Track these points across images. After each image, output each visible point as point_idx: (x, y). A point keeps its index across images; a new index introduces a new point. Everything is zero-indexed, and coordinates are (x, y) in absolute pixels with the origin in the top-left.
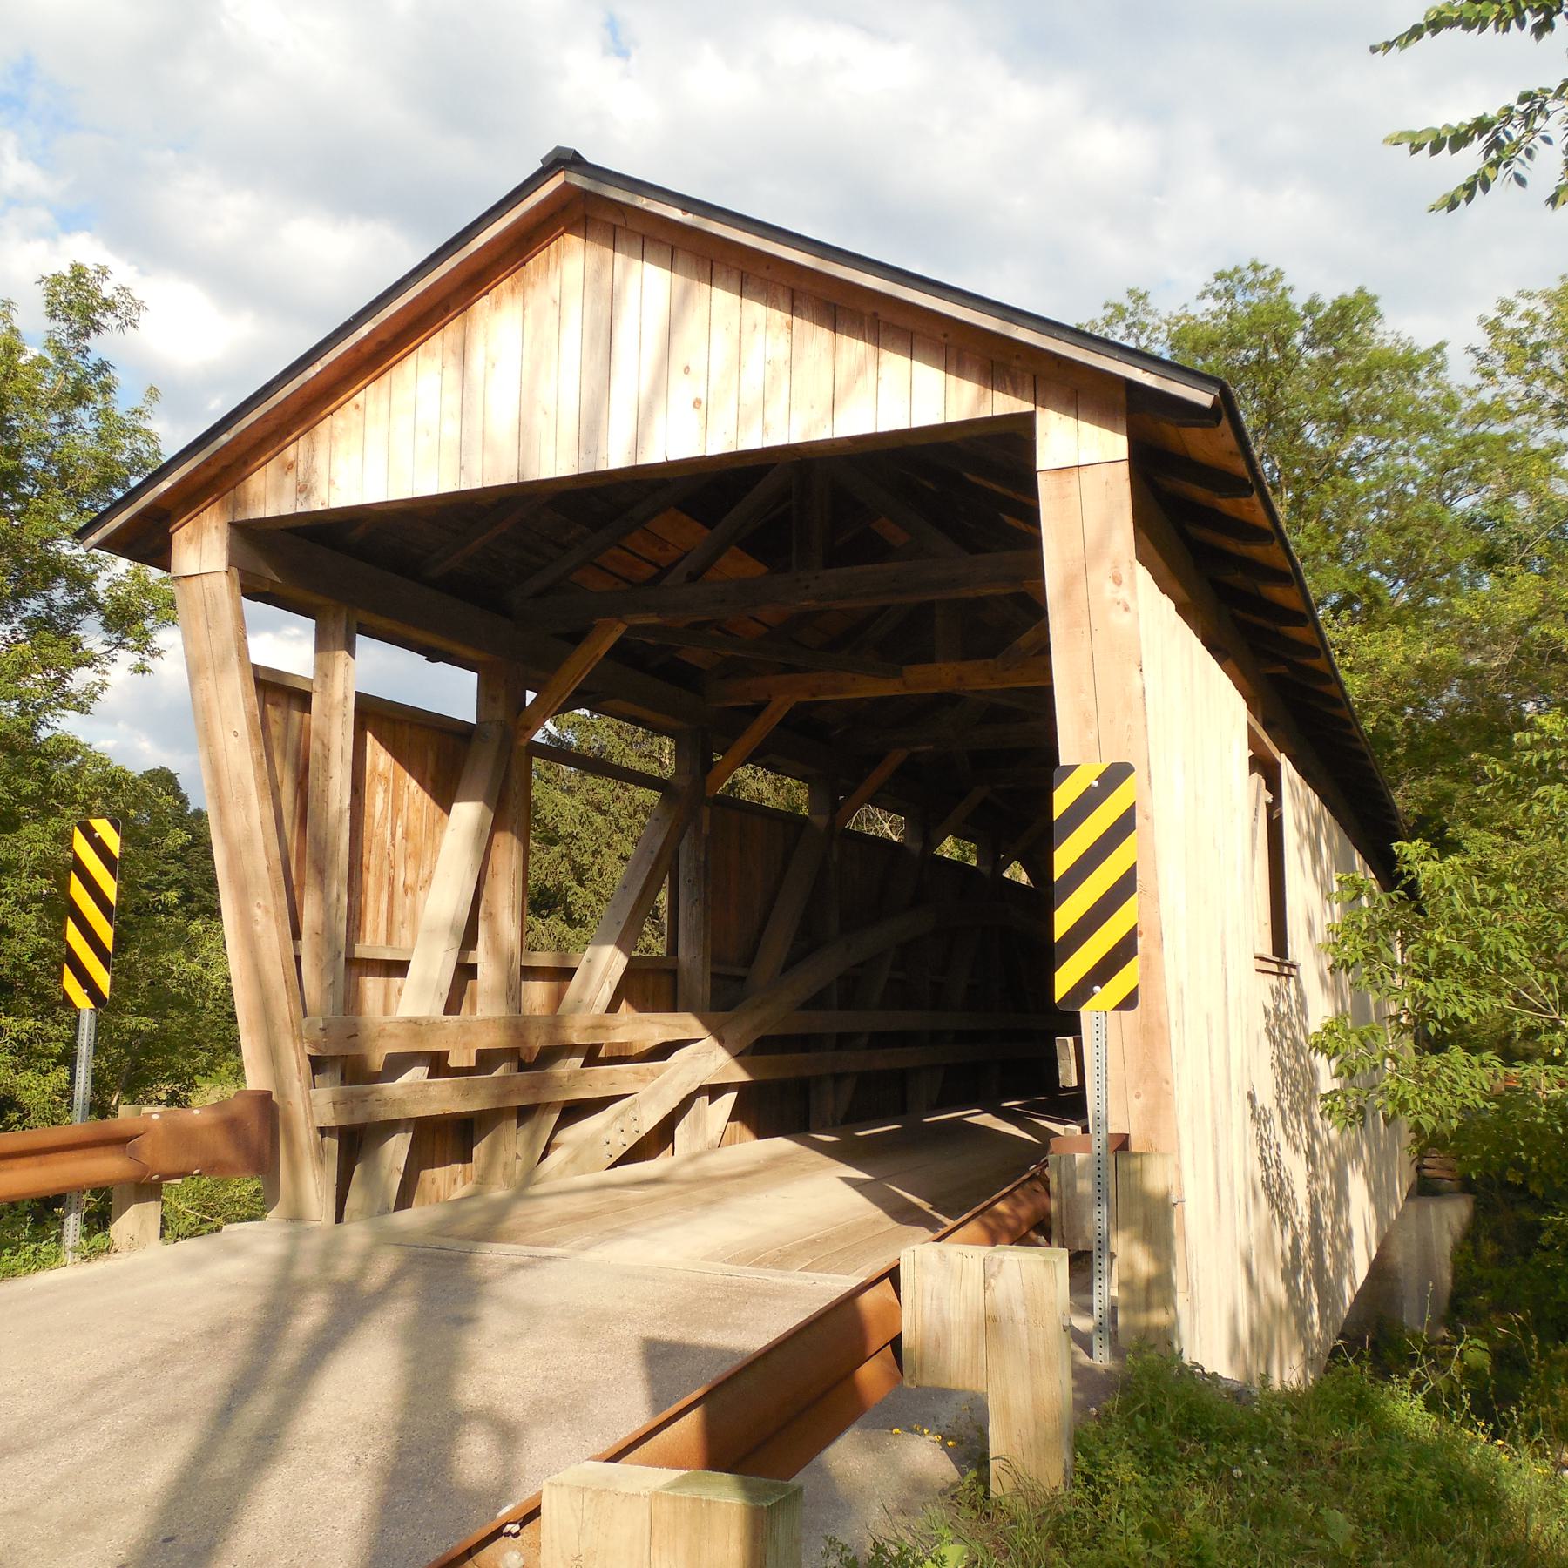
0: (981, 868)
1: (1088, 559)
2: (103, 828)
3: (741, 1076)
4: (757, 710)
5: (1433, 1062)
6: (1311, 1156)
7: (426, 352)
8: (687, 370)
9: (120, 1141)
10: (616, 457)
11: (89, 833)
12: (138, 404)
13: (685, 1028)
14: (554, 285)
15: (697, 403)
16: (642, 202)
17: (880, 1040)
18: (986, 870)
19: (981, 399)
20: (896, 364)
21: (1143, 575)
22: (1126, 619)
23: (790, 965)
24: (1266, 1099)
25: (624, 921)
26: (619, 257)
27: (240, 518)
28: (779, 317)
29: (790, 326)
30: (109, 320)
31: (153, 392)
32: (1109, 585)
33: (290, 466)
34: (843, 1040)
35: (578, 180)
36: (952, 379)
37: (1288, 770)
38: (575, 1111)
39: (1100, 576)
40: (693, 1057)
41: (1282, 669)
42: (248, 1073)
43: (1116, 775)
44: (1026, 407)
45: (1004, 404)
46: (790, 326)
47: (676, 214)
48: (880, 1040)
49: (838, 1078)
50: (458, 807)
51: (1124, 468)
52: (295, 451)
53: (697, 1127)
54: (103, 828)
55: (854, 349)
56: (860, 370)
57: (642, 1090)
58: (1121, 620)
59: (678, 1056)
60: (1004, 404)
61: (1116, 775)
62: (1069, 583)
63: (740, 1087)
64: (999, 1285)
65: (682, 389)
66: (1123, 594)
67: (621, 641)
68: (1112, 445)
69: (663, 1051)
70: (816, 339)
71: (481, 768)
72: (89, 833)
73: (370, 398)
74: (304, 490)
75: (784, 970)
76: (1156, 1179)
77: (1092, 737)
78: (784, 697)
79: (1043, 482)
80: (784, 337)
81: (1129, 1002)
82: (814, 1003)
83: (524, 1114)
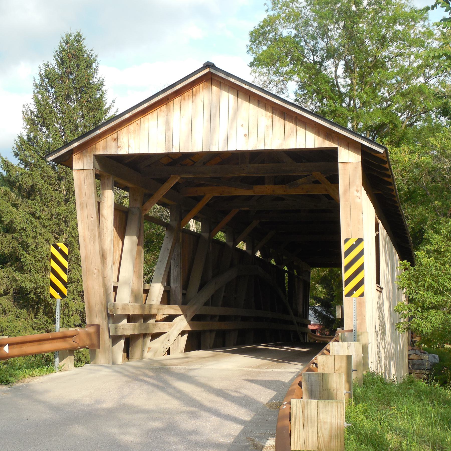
0: (248, 251)
2: (62, 246)
3: (189, 329)
4: (198, 199)
5: (426, 314)
6: (385, 353)
8: (242, 125)
15: (245, 135)
17: (223, 318)
18: (250, 252)
21: (363, 188)
22: (359, 201)
23: (201, 288)
28: (269, 114)
32: (355, 192)
36: (317, 137)
37: (381, 226)
38: (155, 336)
41: (381, 192)
43: (360, 241)
47: (246, 87)
48: (223, 318)
49: (211, 331)
54: (62, 246)
55: (290, 125)
56: (292, 132)
57: (170, 331)
62: (345, 191)
63: (189, 333)
66: (358, 194)
69: (170, 318)
70: (278, 121)
72: (56, 247)
77: (350, 229)
79: (339, 164)
80: (270, 120)
81: (362, 295)
82: (206, 304)
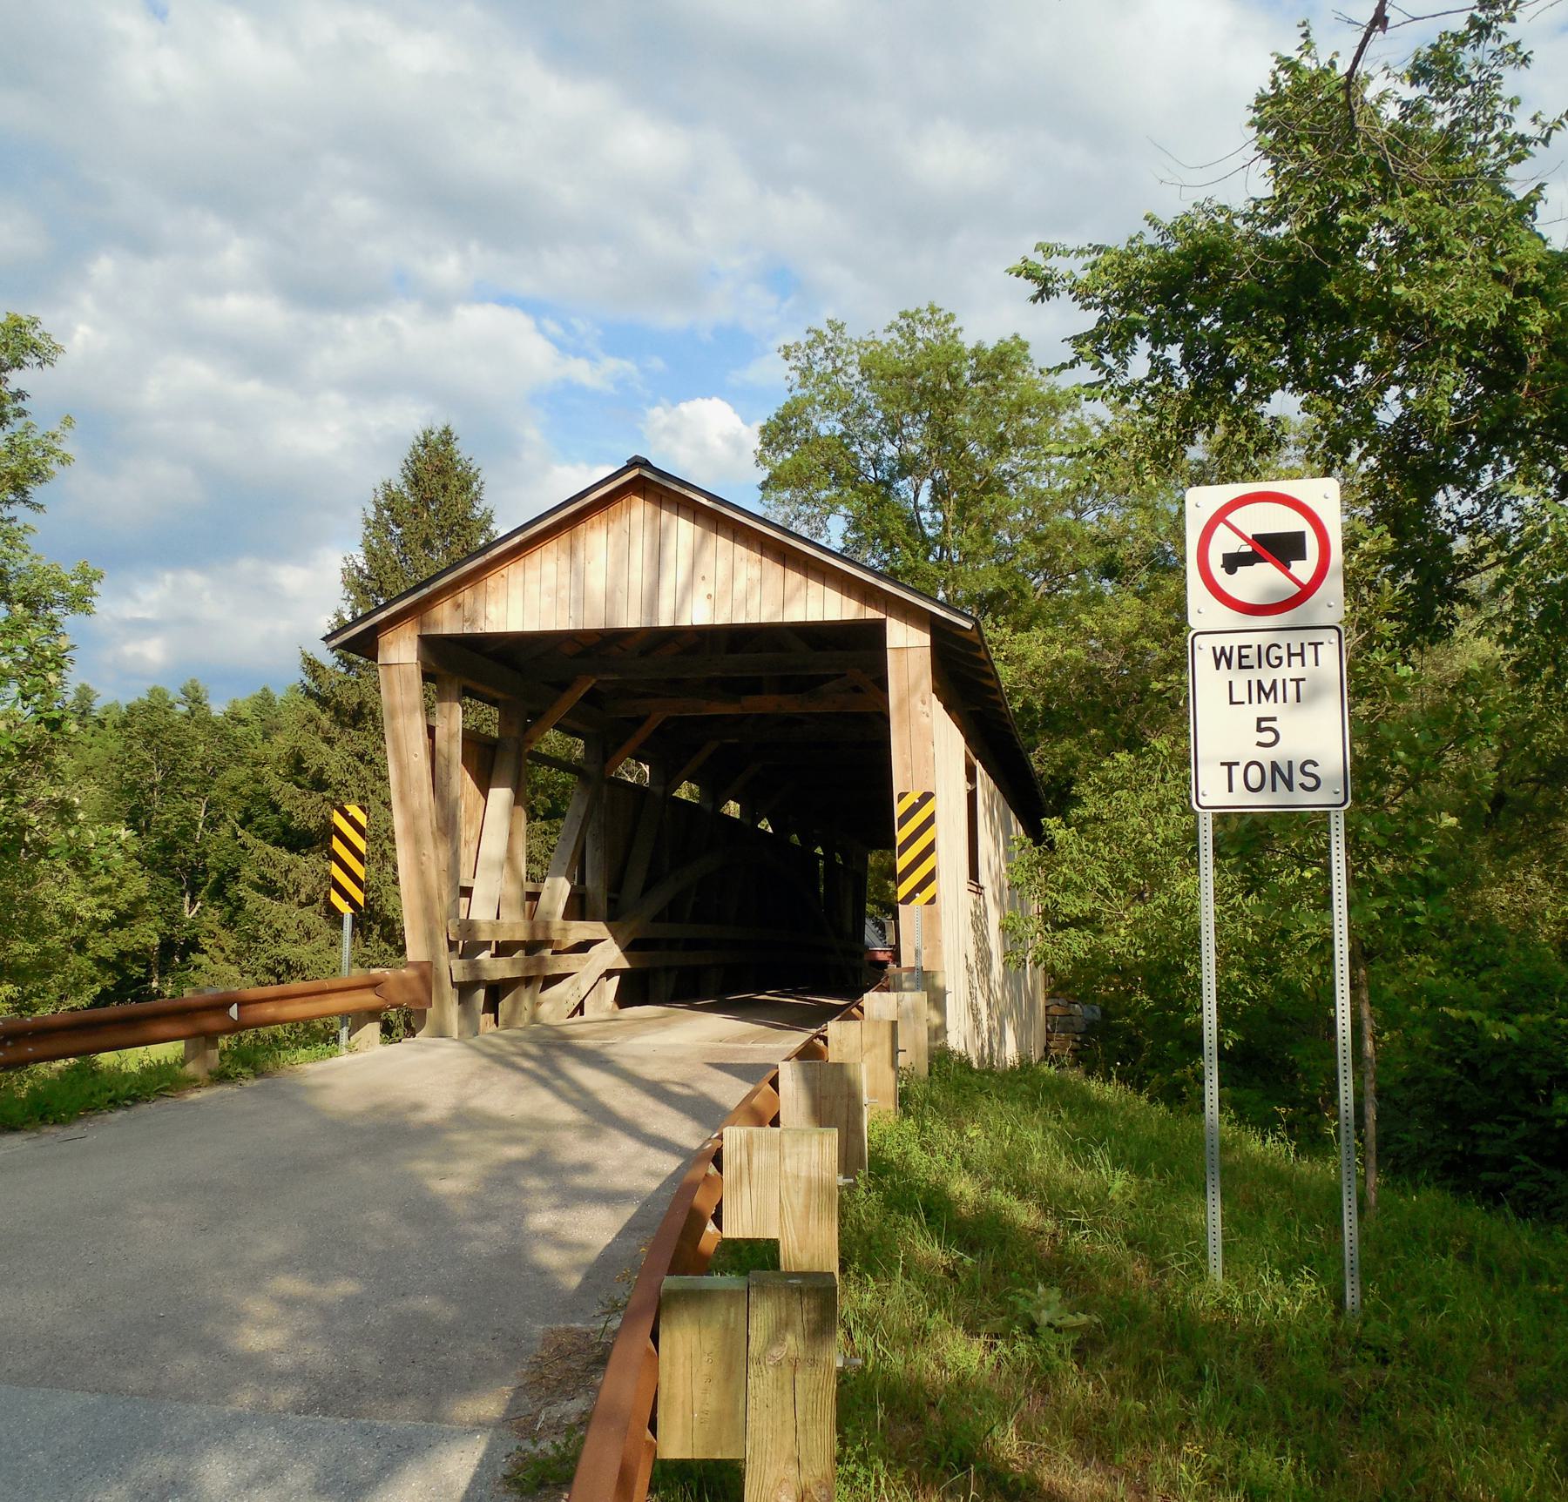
0: (744, 821)
1: (911, 690)
2: (354, 810)
3: (626, 965)
4: (639, 722)
5: (1059, 935)
6: (989, 1004)
7: (547, 550)
8: (703, 578)
9: (374, 985)
10: (665, 621)
11: (344, 813)
12: (55, 428)
13: (600, 931)
14: (625, 522)
15: (709, 596)
16: (686, 492)
17: (692, 945)
18: (747, 821)
19: (860, 610)
20: (815, 588)
22: (927, 720)
23: (647, 888)
24: (972, 960)
25: (569, 860)
26: (664, 512)
27: (425, 633)
28: (757, 556)
29: (761, 562)
30: (31, 359)
31: (68, 421)
32: (920, 704)
33: (459, 606)
34: (671, 944)
35: (647, 474)
36: (845, 598)
37: (980, 768)
39: (916, 701)
40: (603, 950)
41: (978, 708)
42: (408, 951)
43: (927, 797)
44: (883, 616)
45: (872, 614)
46: (761, 562)
48: (692, 945)
49: (668, 969)
50: (492, 791)
51: (928, 650)
52: (466, 595)
53: (600, 997)
54: (354, 810)
55: (794, 577)
56: (798, 589)
57: (581, 970)
58: (925, 720)
59: (594, 950)
60: (872, 614)
61: (927, 797)
62: (901, 702)
63: (622, 972)
64: (903, 1004)
65: (702, 589)
66: (926, 709)
67: (592, 688)
68: (923, 639)
69: (584, 947)
70: (774, 570)
71: (506, 766)
72: (344, 813)
73: (511, 573)
74: (472, 620)
75: (642, 895)
76: (939, 982)
77: (909, 775)
78: (659, 713)
79: (889, 652)
80: (757, 567)
81: (932, 901)
82: (657, 918)
83: (528, 981)
